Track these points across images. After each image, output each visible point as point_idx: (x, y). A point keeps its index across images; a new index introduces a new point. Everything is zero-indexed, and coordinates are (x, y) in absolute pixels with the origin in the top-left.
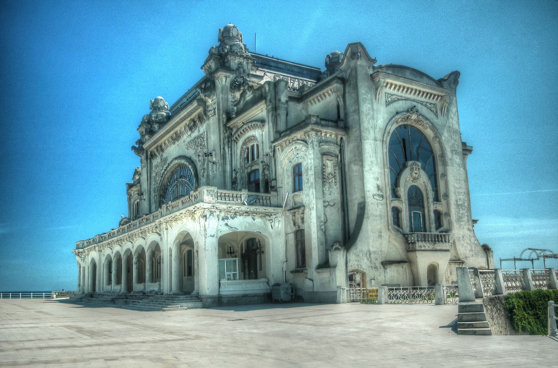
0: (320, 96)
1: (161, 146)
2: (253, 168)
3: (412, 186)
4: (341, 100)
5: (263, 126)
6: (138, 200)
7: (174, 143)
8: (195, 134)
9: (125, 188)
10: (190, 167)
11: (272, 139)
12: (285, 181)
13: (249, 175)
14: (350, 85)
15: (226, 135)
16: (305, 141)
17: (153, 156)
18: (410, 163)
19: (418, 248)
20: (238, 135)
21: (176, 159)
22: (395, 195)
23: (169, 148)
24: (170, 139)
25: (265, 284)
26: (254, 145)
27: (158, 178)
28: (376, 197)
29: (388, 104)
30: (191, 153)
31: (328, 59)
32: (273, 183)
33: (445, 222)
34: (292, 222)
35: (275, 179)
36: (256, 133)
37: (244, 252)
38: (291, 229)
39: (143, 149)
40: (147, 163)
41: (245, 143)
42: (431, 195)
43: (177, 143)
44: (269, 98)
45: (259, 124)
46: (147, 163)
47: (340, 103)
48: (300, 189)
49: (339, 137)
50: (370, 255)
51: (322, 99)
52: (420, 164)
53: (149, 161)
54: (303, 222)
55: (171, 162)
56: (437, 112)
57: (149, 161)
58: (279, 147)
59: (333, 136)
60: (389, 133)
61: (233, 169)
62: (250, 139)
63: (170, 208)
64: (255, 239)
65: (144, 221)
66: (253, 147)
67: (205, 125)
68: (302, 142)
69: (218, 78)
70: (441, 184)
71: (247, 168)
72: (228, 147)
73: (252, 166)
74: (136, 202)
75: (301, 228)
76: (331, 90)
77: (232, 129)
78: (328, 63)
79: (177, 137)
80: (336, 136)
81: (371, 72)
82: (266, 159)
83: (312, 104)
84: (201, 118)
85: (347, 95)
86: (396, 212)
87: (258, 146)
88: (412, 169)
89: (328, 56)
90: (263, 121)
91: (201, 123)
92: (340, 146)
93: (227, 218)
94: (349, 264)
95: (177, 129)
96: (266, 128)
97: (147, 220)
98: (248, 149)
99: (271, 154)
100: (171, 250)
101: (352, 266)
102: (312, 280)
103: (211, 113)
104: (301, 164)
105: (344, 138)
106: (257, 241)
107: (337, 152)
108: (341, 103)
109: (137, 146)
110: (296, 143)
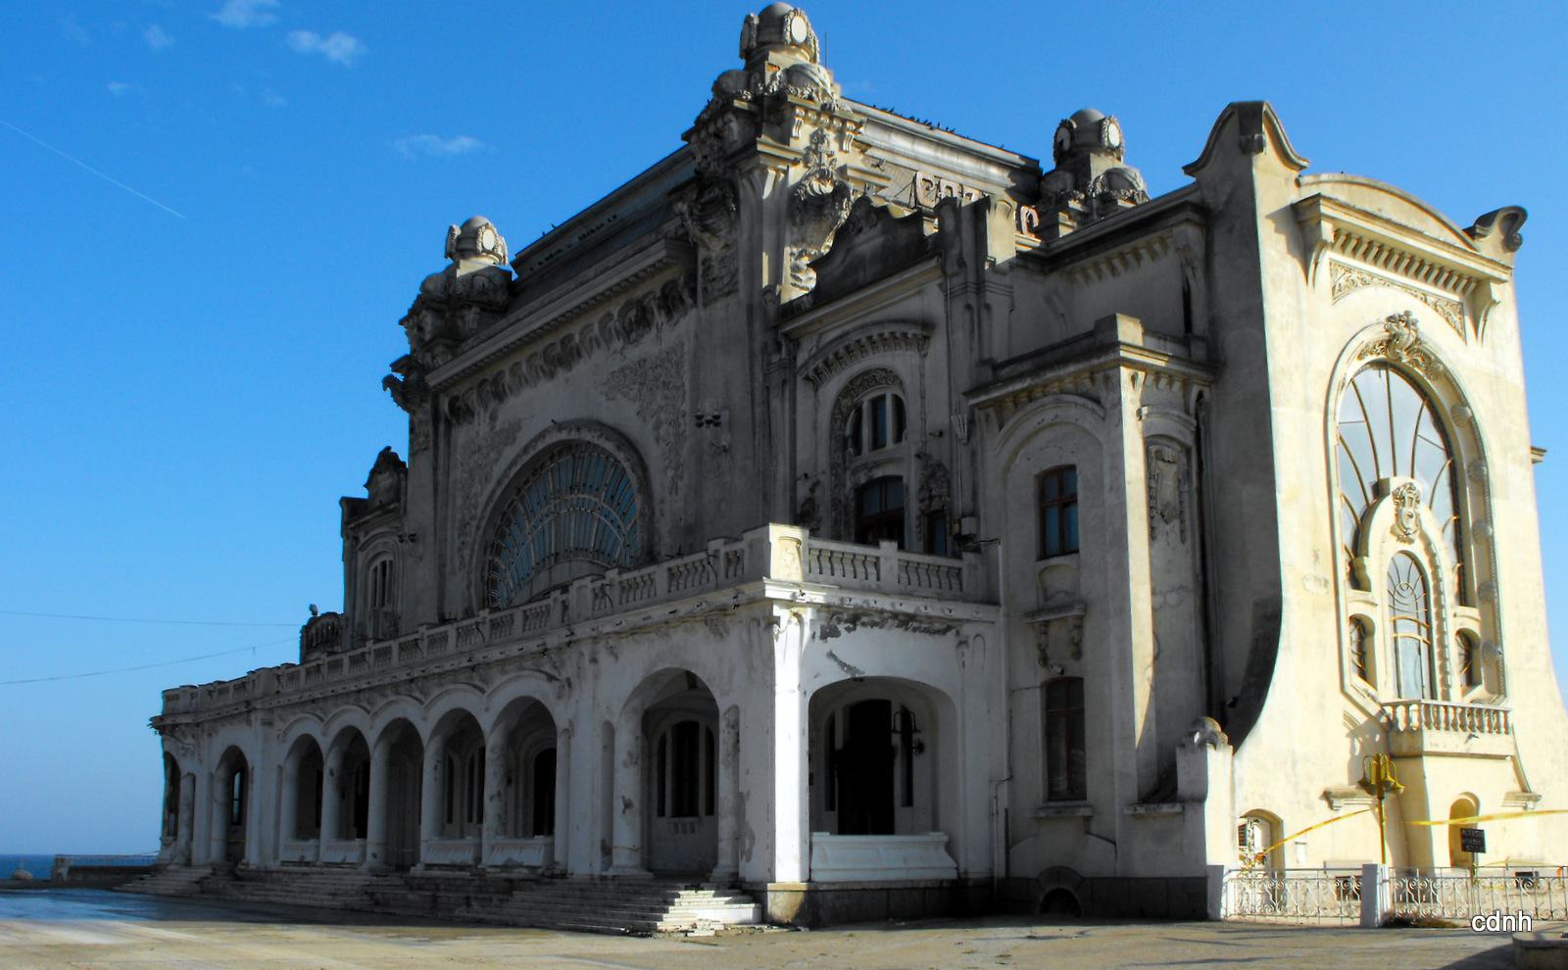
0: (1122, 256)
1: (497, 380)
2: (879, 473)
4: (1200, 274)
5: (926, 338)
6: (387, 558)
7: (552, 375)
8: (634, 353)
9: (336, 515)
10: (621, 456)
11: (964, 382)
13: (861, 491)
14: (1230, 230)
15: (775, 358)
16: (1097, 401)
17: (460, 413)
19: (1427, 748)
20: (826, 362)
21: (559, 426)
22: (1358, 581)
23: (527, 393)
24: (539, 362)
25: (942, 852)
26: (883, 398)
27: (476, 488)
28: (1310, 584)
29: (1337, 292)
30: (624, 413)
31: (1065, 134)
34: (1035, 654)
35: (974, 514)
36: (901, 361)
37: (839, 744)
38: (1033, 678)
39: (426, 389)
40: (436, 434)
41: (847, 391)
43: (561, 374)
44: (955, 252)
45: (911, 331)
46: (436, 434)
47: (1192, 282)
48: (1068, 548)
49: (1195, 390)
50: (1294, 765)
51: (1126, 264)
53: (442, 428)
54: (1078, 654)
55: (542, 435)
56: (1463, 328)
57: (442, 428)
58: (991, 411)
59: (1177, 385)
61: (800, 472)
62: (867, 379)
63: (614, 593)
64: (887, 704)
65: (486, 629)
66: (877, 404)
67: (688, 323)
68: (1080, 400)
69: (750, 171)
71: (855, 472)
72: (783, 401)
73: (877, 465)
74: (377, 563)
75: (1068, 674)
76: (1162, 241)
77: (794, 342)
78: (1066, 145)
79: (565, 357)
80: (1186, 384)
82: (938, 451)
83: (1087, 277)
84: (670, 302)
85: (1218, 261)
87: (898, 403)
88: (1400, 499)
90: (927, 326)
91: (669, 314)
92: (1197, 418)
93: (835, 633)
94: (1240, 793)
95: (575, 330)
96: (938, 345)
97: (495, 625)
98: (859, 411)
99: (962, 433)
100: (610, 730)
101: (1246, 799)
102: (1114, 843)
103: (717, 285)
104: (1072, 468)
105: (1206, 391)
106: (895, 708)
107: (1190, 440)
108: (1198, 287)
109: (400, 377)
110: (1058, 402)
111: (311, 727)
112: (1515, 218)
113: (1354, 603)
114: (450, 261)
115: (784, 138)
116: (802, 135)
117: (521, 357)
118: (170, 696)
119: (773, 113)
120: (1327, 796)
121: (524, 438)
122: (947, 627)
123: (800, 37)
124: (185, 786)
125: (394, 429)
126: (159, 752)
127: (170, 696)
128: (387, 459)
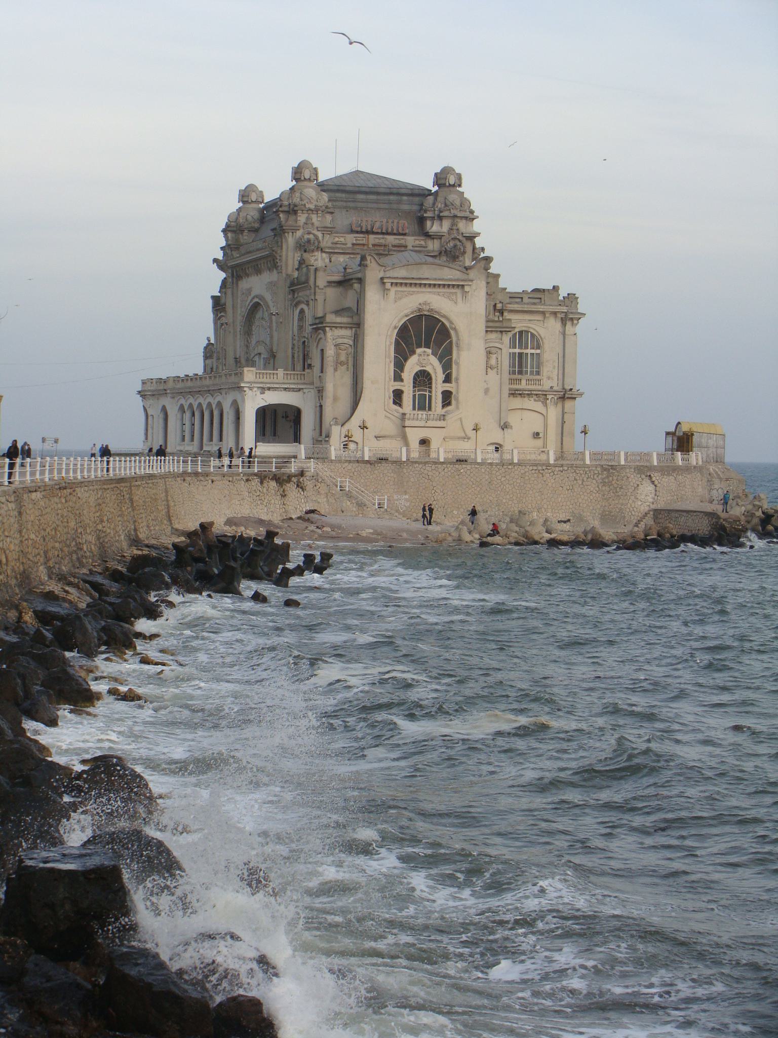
3: (420, 371)
9: (210, 303)
12: (316, 363)
17: (239, 278)
18: (419, 351)
21: (257, 296)
30: (268, 297)
32: (309, 362)
33: (453, 402)
52: (429, 351)
55: (253, 298)
60: (395, 328)
70: (454, 366)
77: (293, 291)
79: (258, 271)
81: (381, 275)
89: (436, 174)
93: (263, 393)
107: (351, 343)
114: (241, 204)
115: (296, 221)
116: (302, 218)
118: (144, 383)
119: (293, 211)
120: (376, 437)
121: (252, 296)
122: (299, 390)
123: (307, 177)
124: (150, 418)
125: (223, 275)
126: (141, 404)
128: (224, 284)
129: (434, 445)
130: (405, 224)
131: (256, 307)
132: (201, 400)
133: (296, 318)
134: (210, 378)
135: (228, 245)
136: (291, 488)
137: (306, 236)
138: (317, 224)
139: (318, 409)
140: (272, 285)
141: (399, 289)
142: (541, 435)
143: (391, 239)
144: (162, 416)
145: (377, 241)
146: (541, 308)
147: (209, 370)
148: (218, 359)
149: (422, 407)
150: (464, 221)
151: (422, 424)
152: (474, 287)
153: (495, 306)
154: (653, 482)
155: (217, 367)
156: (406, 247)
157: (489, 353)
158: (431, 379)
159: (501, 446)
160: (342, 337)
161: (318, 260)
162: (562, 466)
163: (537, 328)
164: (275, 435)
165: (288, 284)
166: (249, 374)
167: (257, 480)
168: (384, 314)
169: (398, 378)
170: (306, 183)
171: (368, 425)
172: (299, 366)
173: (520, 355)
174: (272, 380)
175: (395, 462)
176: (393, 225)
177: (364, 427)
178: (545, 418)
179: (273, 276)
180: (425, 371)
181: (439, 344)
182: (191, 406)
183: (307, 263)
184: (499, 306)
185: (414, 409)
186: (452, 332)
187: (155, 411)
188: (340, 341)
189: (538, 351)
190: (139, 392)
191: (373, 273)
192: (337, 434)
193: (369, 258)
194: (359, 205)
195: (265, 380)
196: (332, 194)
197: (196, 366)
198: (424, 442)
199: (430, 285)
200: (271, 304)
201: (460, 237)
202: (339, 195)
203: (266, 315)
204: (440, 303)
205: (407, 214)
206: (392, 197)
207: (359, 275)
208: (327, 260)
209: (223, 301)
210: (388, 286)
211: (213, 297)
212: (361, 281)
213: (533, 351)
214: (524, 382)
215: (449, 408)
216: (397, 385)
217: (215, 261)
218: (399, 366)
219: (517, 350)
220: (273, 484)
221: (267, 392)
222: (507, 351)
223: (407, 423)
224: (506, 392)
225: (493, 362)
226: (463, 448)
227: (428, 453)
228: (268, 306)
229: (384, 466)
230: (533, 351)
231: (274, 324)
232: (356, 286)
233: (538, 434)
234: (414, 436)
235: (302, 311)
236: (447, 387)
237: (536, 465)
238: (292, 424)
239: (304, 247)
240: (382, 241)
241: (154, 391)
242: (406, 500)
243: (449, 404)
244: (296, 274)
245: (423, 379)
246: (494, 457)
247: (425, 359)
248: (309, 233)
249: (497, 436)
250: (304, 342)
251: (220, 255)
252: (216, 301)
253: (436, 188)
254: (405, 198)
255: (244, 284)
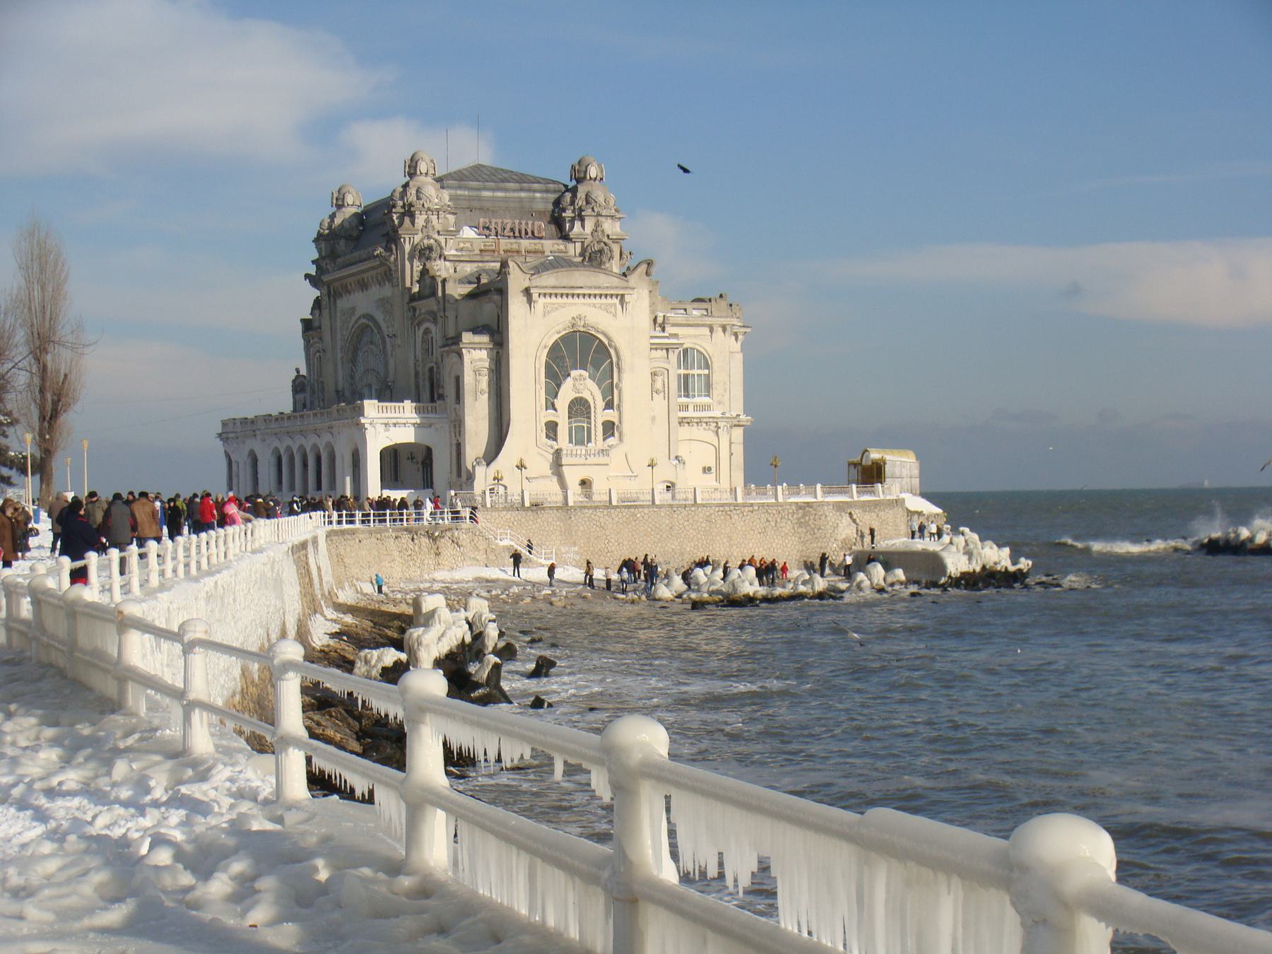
3: (576, 399)
9: (299, 327)
12: (449, 391)
18: (574, 373)
21: (364, 316)
30: (379, 316)
32: (441, 391)
42: (600, 404)
52: (585, 374)
70: (616, 392)
77: (415, 310)
79: (363, 286)
81: (527, 284)
86: (552, 428)
88: (575, 379)
111: (276, 443)
112: (650, 264)
113: (550, 415)
116: (420, 220)
117: (350, 280)
118: (224, 424)
121: (358, 314)
123: (424, 171)
124: (234, 466)
125: (317, 293)
126: (222, 450)
127: (224, 424)
128: (317, 304)
129: (595, 487)
130: (542, 225)
131: (363, 329)
132: (300, 440)
133: (419, 340)
134: (315, 415)
135: (322, 258)
136: (445, 543)
137: (426, 241)
138: (438, 227)
139: (454, 447)
140: (383, 303)
141: (548, 300)
142: (713, 470)
143: (525, 244)
144: (249, 461)
145: (509, 247)
146: (708, 321)
147: (299, 406)
148: (313, 392)
149: (580, 442)
150: (610, 221)
151: (582, 461)
152: (635, 296)
153: (655, 320)
154: (854, 521)
155: (312, 403)
156: (543, 252)
157: (654, 374)
158: (589, 407)
159: (673, 484)
160: (481, 360)
161: (441, 269)
162: (752, 505)
163: (704, 344)
164: (396, 479)
165: (407, 300)
166: (371, 408)
167: (406, 537)
168: (532, 328)
169: (551, 406)
170: (422, 178)
171: (526, 463)
172: (426, 394)
173: (686, 377)
174: (397, 415)
175: (558, 508)
176: (529, 225)
177: (521, 466)
178: (717, 451)
179: (387, 291)
180: (581, 398)
181: (597, 366)
182: (289, 449)
183: (431, 273)
184: (660, 320)
185: (571, 441)
186: (612, 351)
187: (241, 457)
188: (480, 364)
189: (706, 372)
190: (220, 435)
191: (516, 281)
192: (482, 478)
193: (511, 264)
194: (487, 205)
195: (389, 415)
196: (453, 192)
197: (285, 403)
198: (583, 483)
199: (584, 295)
200: (383, 325)
201: (605, 239)
202: (459, 192)
203: (377, 338)
204: (598, 316)
205: (540, 214)
206: (523, 194)
207: (499, 285)
208: (452, 271)
209: (316, 324)
210: (535, 296)
211: (303, 321)
212: (502, 291)
213: (700, 372)
214: (691, 408)
215: (611, 441)
216: (550, 415)
217: (307, 276)
218: (552, 393)
219: (682, 371)
220: (425, 541)
221: (392, 428)
222: (676, 372)
223: (564, 461)
224: (674, 422)
225: (659, 385)
226: (632, 487)
227: (589, 496)
228: (379, 328)
229: (545, 515)
230: (700, 372)
231: (389, 348)
232: (496, 297)
233: (709, 469)
234: (573, 476)
235: (427, 331)
236: (611, 415)
237: (723, 505)
238: (420, 466)
239: (424, 253)
240: (515, 247)
241: (234, 431)
242: (577, 553)
243: (613, 435)
244: (416, 289)
245: (579, 408)
246: (662, 497)
247: (580, 384)
248: (429, 237)
249: (666, 471)
250: (431, 369)
251: (312, 270)
252: (307, 325)
253: (574, 183)
254: (538, 195)
255: (343, 303)
